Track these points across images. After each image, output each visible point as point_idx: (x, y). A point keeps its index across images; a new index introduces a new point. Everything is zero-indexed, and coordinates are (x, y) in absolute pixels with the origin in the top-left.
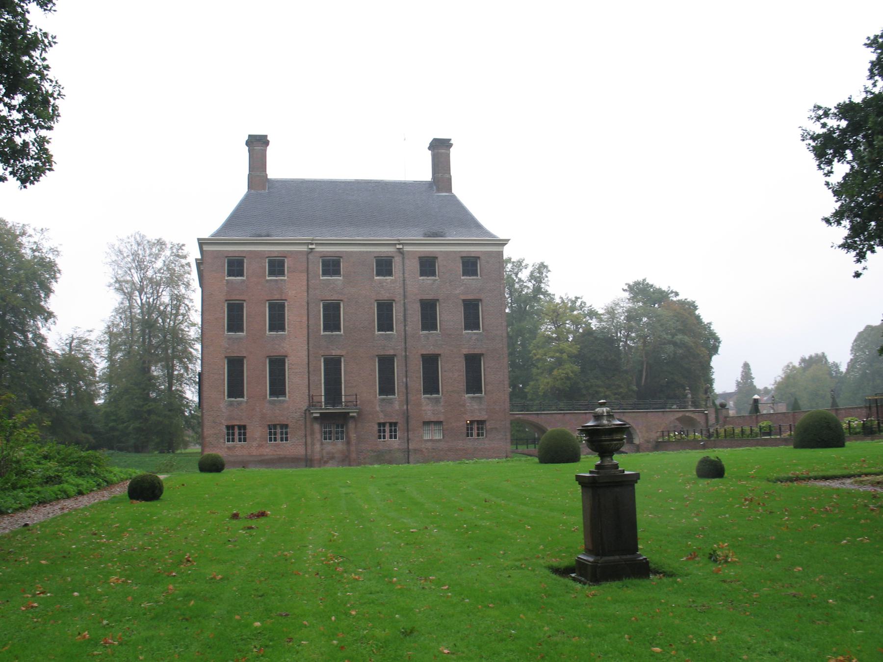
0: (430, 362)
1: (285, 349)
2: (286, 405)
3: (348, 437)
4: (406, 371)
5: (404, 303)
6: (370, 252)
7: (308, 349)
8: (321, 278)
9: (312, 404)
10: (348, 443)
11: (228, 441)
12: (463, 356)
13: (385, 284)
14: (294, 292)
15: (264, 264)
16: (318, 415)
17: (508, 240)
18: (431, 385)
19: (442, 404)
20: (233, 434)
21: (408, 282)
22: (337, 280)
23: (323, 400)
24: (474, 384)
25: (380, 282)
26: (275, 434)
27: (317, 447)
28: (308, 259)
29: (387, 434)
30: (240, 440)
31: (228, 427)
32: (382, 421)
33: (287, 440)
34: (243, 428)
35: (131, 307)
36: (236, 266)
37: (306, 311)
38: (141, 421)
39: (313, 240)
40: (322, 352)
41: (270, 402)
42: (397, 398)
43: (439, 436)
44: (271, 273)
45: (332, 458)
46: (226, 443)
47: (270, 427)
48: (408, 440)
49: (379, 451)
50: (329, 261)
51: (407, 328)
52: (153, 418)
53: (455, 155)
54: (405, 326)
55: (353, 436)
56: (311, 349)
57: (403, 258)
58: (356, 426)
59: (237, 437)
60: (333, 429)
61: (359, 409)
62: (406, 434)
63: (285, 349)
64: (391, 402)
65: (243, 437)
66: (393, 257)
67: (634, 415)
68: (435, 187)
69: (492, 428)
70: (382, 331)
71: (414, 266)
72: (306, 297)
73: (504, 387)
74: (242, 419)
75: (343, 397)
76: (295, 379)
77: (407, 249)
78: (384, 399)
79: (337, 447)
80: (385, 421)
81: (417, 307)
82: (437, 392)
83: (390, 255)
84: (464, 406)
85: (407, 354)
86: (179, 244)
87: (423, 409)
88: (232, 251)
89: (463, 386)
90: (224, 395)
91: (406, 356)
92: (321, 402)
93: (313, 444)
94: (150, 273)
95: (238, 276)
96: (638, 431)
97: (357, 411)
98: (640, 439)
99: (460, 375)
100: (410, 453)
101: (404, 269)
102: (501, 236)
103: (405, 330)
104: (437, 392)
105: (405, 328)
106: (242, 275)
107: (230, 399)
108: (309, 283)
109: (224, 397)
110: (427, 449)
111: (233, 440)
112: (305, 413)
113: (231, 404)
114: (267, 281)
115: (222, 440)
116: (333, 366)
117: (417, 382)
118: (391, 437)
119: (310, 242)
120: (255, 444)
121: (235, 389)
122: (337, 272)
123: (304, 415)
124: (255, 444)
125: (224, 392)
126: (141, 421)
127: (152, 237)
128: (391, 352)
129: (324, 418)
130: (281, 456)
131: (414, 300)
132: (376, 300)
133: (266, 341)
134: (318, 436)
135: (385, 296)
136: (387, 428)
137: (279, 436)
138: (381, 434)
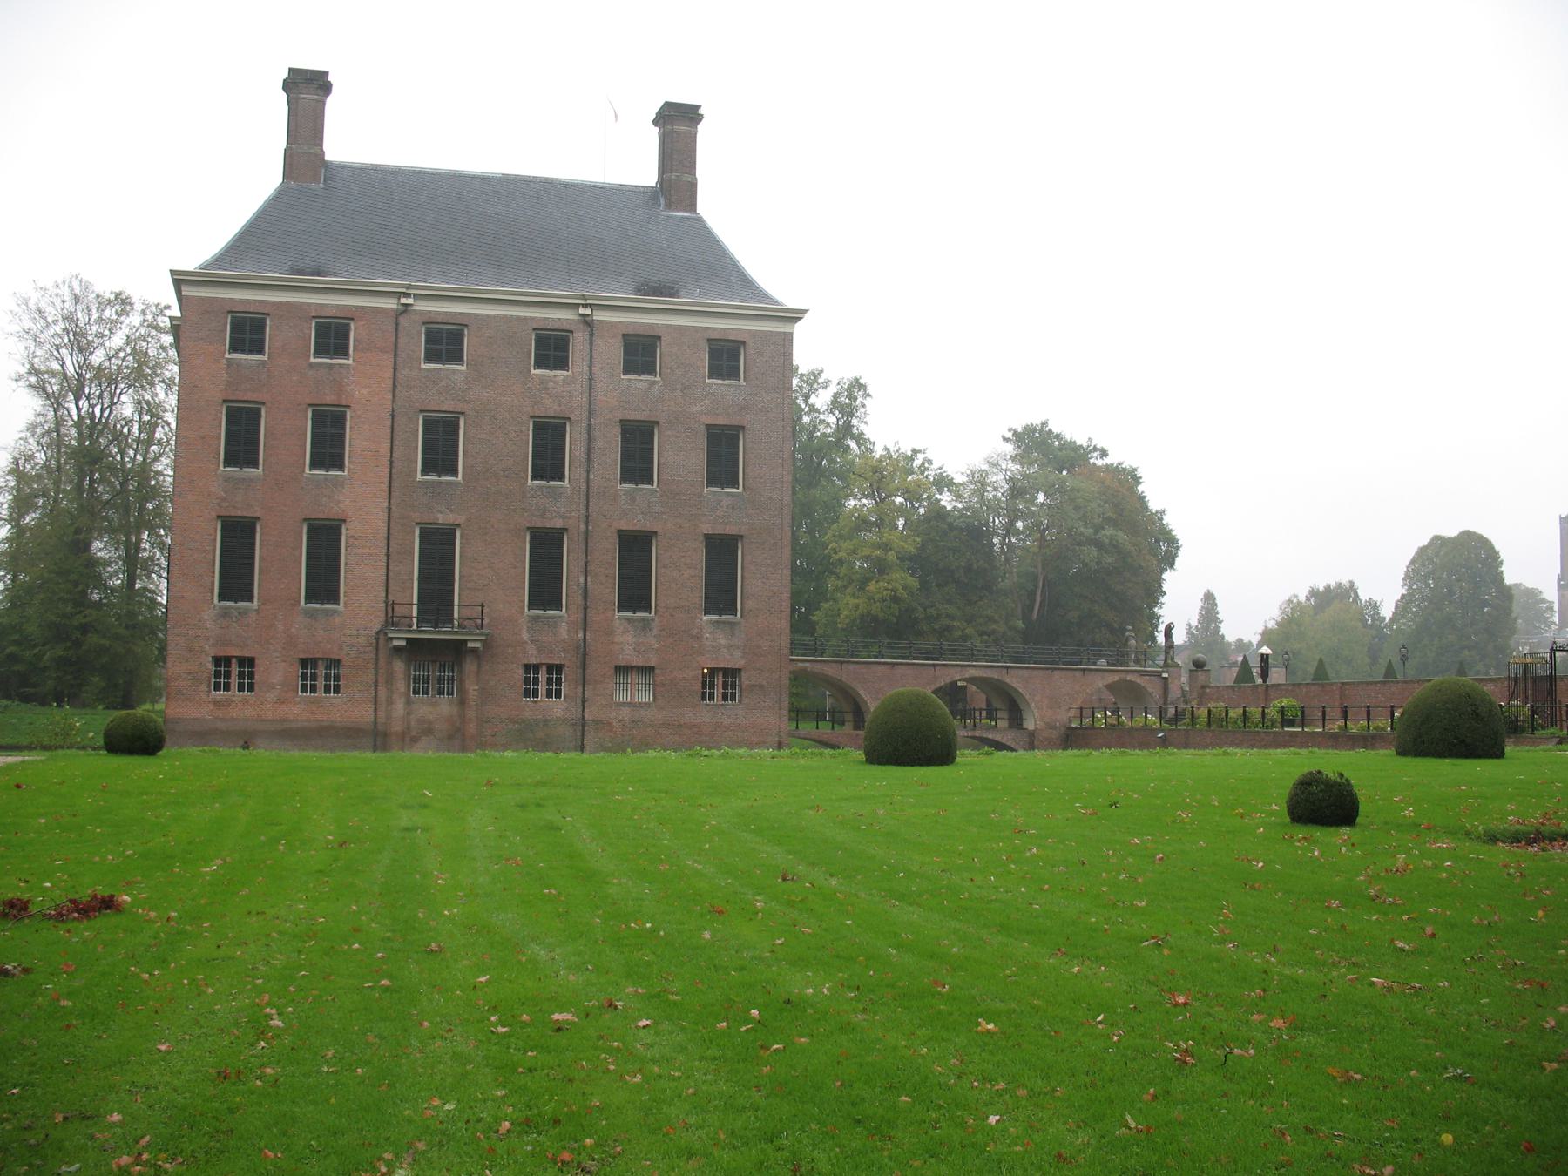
0: (636, 547)
1: (341, 505)
2: (338, 620)
3: (462, 691)
4: (586, 563)
5: (589, 425)
6: (525, 318)
7: (389, 509)
8: (423, 366)
9: (391, 621)
10: (462, 702)
11: (217, 688)
12: (702, 538)
13: (551, 384)
14: (365, 391)
15: (307, 331)
16: (403, 643)
17: (804, 312)
18: (635, 594)
19: (655, 632)
20: (228, 675)
21: (598, 384)
22: (454, 372)
23: (415, 613)
24: (720, 596)
25: (543, 381)
26: (314, 678)
27: (399, 707)
28: (397, 324)
29: (542, 688)
30: (241, 688)
31: (217, 661)
32: (533, 661)
33: (337, 690)
34: (248, 662)
35: (59, 422)
37: (389, 431)
38: (69, 644)
39: (410, 286)
40: (416, 517)
41: (306, 612)
42: (566, 615)
43: (644, 697)
44: (321, 350)
45: (429, 731)
46: (213, 692)
47: (304, 663)
48: (583, 702)
49: (523, 721)
50: (440, 331)
51: (592, 477)
52: (93, 639)
53: (708, 140)
54: (588, 472)
55: (472, 688)
56: (393, 508)
57: (591, 335)
58: (479, 666)
59: (234, 681)
60: (433, 673)
61: (487, 634)
62: (580, 689)
63: (341, 505)
64: (552, 624)
65: (248, 682)
66: (572, 332)
67: (1026, 672)
68: (662, 201)
69: (753, 685)
70: (542, 479)
71: (611, 352)
72: (390, 403)
73: (781, 605)
74: (247, 646)
75: (456, 608)
77: (599, 316)
79: (440, 709)
80: (539, 662)
81: (616, 434)
82: (648, 609)
83: (565, 326)
84: (698, 638)
85: (590, 528)
86: (158, 304)
87: (616, 640)
88: (241, 301)
89: (698, 597)
90: (212, 593)
91: (587, 531)
92: (411, 617)
93: (390, 702)
94: (98, 358)
95: (251, 352)
96: (1033, 705)
97: (483, 638)
98: (1035, 721)
99: (692, 577)
100: (586, 728)
101: (591, 357)
102: (790, 302)
103: (588, 481)
104: (648, 609)
105: (588, 476)
106: (261, 351)
107: (223, 603)
108: (398, 375)
109: (212, 599)
110: (620, 721)
111: (227, 687)
112: (377, 639)
113: (225, 614)
114: (312, 366)
115: (204, 687)
116: (438, 545)
117: (607, 587)
118: (549, 695)
119: (404, 290)
120: (271, 696)
122: (456, 357)
123: (374, 641)
124: (271, 696)
125: (213, 589)
126: (69, 644)
127: (106, 286)
128: (558, 523)
129: (415, 650)
130: (325, 724)
131: (609, 419)
132: (532, 417)
133: (302, 488)
134: (401, 686)
135: (550, 408)
136: (543, 676)
137: (321, 683)
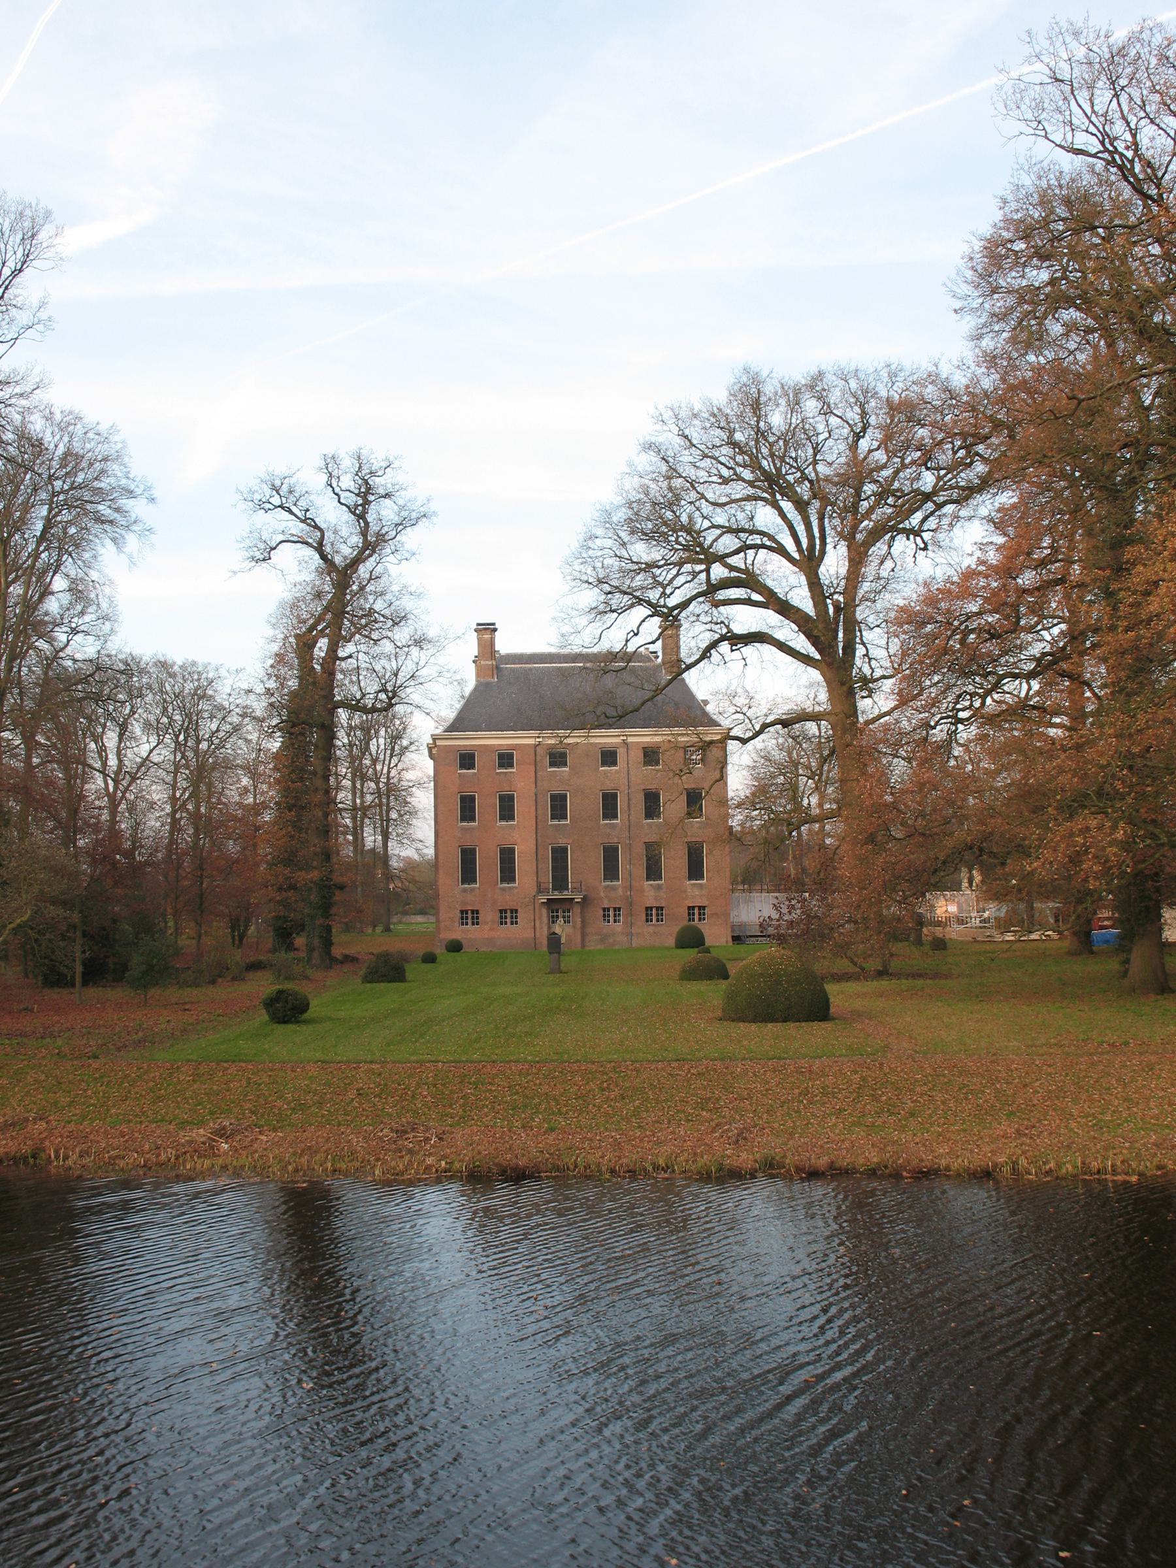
9: (540, 890)
18: (653, 871)
21: (632, 773)
25: (605, 773)
34: (476, 912)
36: (467, 760)
47: (501, 911)
59: (470, 921)
77: (630, 740)
78: (608, 886)
81: (641, 797)
84: (685, 891)
89: (685, 872)
116: (560, 855)
120: (487, 927)
121: (468, 875)
124: (487, 927)
128: (616, 840)
135: (609, 786)
136: (612, 913)
137: (508, 920)
138: (606, 917)
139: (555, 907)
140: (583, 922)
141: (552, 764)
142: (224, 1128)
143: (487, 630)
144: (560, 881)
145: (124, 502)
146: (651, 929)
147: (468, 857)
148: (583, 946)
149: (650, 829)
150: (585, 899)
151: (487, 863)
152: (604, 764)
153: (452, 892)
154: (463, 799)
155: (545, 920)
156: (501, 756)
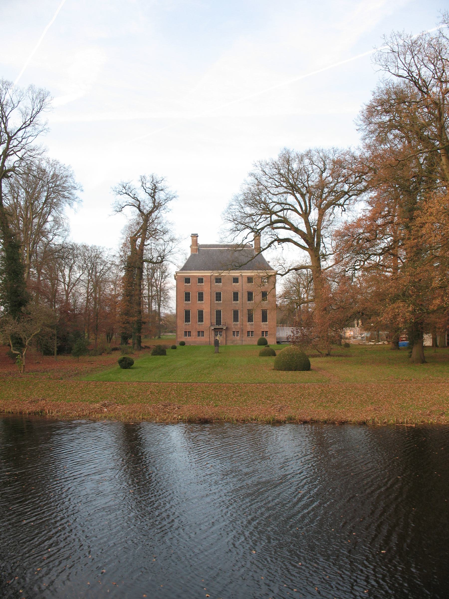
9: (212, 325)
18: (250, 319)
25: (234, 285)
36: (187, 280)
47: (198, 332)
59: (188, 335)
76: (206, 316)
77: (243, 274)
116: (218, 313)
120: (193, 337)
121: (187, 319)
124: (193, 337)
135: (236, 290)
136: (236, 333)
139: (217, 331)
140: (226, 336)
141: (216, 282)
142: (105, 404)
143: (195, 236)
144: (218, 322)
145: (73, 191)
146: (249, 339)
147: (187, 313)
148: (226, 344)
149: (249, 305)
150: (227, 328)
151: (194, 315)
152: (234, 282)
153: (182, 325)
154: (186, 294)
155: (213, 335)
156: (199, 279)
